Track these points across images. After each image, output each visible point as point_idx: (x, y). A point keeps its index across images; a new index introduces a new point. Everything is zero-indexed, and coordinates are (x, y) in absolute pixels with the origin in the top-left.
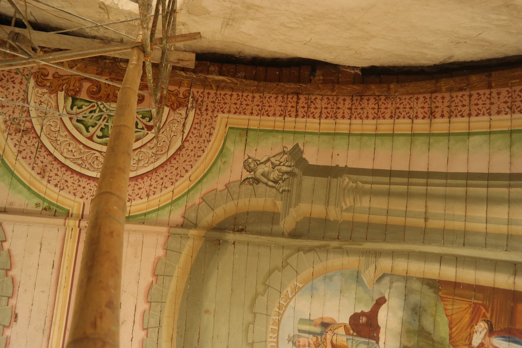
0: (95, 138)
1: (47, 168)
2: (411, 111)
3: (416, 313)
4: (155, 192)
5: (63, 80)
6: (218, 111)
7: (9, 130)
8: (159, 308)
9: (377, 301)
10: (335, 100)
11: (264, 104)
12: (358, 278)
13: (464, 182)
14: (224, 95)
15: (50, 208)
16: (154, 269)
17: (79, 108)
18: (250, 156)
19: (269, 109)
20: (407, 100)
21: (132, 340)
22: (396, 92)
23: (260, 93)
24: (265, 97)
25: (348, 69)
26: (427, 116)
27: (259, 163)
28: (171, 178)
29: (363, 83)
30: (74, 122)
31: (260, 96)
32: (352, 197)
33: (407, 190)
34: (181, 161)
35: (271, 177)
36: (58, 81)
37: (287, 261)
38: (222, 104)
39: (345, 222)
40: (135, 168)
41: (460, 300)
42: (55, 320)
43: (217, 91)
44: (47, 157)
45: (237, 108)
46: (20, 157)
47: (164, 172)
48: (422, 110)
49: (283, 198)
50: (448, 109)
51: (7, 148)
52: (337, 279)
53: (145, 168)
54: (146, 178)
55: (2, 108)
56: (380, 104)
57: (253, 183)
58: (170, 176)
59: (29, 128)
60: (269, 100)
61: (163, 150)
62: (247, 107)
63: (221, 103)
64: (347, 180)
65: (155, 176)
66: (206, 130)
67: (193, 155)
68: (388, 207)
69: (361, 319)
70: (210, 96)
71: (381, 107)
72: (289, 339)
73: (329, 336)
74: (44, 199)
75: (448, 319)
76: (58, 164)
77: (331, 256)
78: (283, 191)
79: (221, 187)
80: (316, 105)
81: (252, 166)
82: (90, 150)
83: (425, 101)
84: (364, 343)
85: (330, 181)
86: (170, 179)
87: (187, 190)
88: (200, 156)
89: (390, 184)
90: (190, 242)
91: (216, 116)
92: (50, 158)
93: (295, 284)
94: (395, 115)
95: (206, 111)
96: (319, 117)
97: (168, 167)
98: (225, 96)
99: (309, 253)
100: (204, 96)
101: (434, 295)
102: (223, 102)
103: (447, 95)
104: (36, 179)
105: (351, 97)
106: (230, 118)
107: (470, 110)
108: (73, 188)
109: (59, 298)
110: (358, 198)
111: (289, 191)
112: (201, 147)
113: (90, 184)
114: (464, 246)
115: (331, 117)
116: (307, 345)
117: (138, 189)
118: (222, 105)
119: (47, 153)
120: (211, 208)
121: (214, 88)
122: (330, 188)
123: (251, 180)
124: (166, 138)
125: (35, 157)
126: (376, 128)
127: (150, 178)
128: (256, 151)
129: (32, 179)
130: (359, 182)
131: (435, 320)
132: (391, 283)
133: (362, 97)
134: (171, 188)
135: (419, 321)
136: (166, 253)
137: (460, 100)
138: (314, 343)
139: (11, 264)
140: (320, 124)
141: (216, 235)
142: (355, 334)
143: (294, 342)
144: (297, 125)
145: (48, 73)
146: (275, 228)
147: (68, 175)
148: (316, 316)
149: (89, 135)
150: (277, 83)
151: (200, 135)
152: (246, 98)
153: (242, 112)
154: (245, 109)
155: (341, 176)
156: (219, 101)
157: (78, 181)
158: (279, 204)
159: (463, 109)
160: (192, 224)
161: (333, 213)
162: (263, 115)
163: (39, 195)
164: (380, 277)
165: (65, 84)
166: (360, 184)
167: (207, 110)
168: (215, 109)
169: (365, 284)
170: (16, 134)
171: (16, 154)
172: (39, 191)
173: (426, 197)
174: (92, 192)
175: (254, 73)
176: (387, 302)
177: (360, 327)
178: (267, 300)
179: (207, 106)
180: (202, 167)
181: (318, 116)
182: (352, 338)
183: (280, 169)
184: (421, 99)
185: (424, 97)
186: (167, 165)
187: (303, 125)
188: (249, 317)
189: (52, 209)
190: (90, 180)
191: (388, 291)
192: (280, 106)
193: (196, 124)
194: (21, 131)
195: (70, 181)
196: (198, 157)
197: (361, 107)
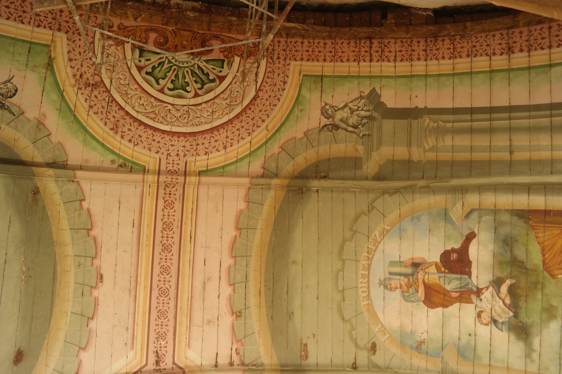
0: (166, 91)
1: (119, 123)
2: (488, 48)
3: (507, 244)
4: (232, 144)
5: (128, 32)
6: (290, 59)
7: (79, 84)
8: (244, 263)
9: (466, 236)
10: (409, 43)
11: (337, 51)
12: (446, 216)
13: (548, 112)
14: (295, 43)
15: (125, 165)
16: (237, 222)
17: (147, 60)
18: (327, 102)
19: (343, 55)
20: (483, 38)
22: (471, 31)
23: (331, 39)
24: (337, 43)
25: (420, 11)
26: (505, 52)
27: (336, 109)
28: (247, 129)
29: (436, 24)
30: (143, 73)
31: (332, 42)
32: (434, 137)
33: (489, 126)
34: (257, 111)
35: (351, 122)
36: (124, 32)
37: (373, 204)
38: (294, 51)
39: (429, 162)
40: (210, 120)
41: (552, 227)
42: (140, 280)
43: (287, 38)
44: (119, 112)
45: (309, 55)
46: (91, 113)
47: (240, 122)
48: (500, 47)
49: (364, 142)
50: (526, 43)
51: (78, 103)
52: (425, 219)
53: (220, 120)
54: (221, 130)
55: (71, 62)
56: (455, 44)
57: (332, 129)
58: (246, 127)
59: (99, 82)
60: (342, 46)
61: (237, 100)
62: (320, 54)
63: (292, 51)
64: (428, 120)
65: (231, 128)
66: (280, 78)
67: (268, 104)
68: (471, 144)
69: (452, 255)
70: (281, 44)
71: (457, 47)
72: (380, 283)
73: (420, 276)
74: (119, 156)
75: (540, 246)
76: (130, 118)
77: (417, 196)
78: (364, 135)
79: (300, 135)
80: (390, 49)
81: (330, 112)
82: (162, 103)
83: (502, 37)
84: (457, 279)
85: (411, 122)
86: (246, 129)
87: (265, 140)
88: (276, 105)
89: (472, 121)
90: (272, 193)
91: (288, 64)
92: (122, 113)
93: (383, 227)
94: (472, 53)
95: (278, 60)
96: (394, 60)
97: (244, 118)
98: (296, 44)
99: (394, 196)
100: (274, 45)
101: (524, 225)
102: (295, 49)
103: (525, 30)
104: (109, 134)
105: (425, 39)
106: (303, 66)
107: (550, 42)
108: (147, 143)
109: (142, 257)
110: (440, 137)
111: (369, 135)
112: (276, 96)
114: (552, 174)
115: (407, 60)
116: (399, 287)
117: (215, 141)
118: (294, 53)
120: (291, 156)
121: (284, 36)
122: (410, 129)
123: (330, 126)
124: (239, 88)
125: (107, 112)
126: (453, 67)
127: (226, 129)
128: (332, 97)
129: (105, 135)
130: (440, 122)
131: (527, 249)
132: (480, 217)
133: (437, 38)
134: (248, 139)
135: (511, 252)
137: (539, 33)
138: (406, 284)
140: (395, 67)
141: (299, 182)
142: (447, 271)
143: (385, 285)
144: (373, 69)
145: (113, 24)
146: (358, 173)
147: (142, 130)
148: (407, 257)
149: (159, 87)
150: (349, 28)
151: (274, 83)
152: (317, 45)
153: (315, 59)
154: (318, 55)
155: (421, 117)
156: (291, 49)
157: (152, 135)
158: (361, 148)
159: (543, 42)
160: (273, 175)
161: (416, 154)
162: (337, 61)
163: (114, 151)
164: (468, 213)
165: (131, 35)
166: (441, 124)
167: (278, 58)
168: (287, 57)
169: (454, 221)
170: (86, 88)
171: (88, 109)
172: (114, 147)
173: (510, 130)
175: (323, 19)
176: (477, 237)
177: (452, 263)
178: (355, 246)
179: (279, 54)
180: (279, 116)
181: (393, 59)
182: (444, 275)
183: (359, 114)
184: (498, 36)
185: (501, 34)
186: (242, 115)
187: (378, 69)
188: (339, 265)
189: (127, 166)
190: (165, 134)
191: (477, 226)
192: (354, 51)
193: (268, 72)
194: (91, 85)
195: (144, 136)
196: (274, 105)
197: (436, 48)
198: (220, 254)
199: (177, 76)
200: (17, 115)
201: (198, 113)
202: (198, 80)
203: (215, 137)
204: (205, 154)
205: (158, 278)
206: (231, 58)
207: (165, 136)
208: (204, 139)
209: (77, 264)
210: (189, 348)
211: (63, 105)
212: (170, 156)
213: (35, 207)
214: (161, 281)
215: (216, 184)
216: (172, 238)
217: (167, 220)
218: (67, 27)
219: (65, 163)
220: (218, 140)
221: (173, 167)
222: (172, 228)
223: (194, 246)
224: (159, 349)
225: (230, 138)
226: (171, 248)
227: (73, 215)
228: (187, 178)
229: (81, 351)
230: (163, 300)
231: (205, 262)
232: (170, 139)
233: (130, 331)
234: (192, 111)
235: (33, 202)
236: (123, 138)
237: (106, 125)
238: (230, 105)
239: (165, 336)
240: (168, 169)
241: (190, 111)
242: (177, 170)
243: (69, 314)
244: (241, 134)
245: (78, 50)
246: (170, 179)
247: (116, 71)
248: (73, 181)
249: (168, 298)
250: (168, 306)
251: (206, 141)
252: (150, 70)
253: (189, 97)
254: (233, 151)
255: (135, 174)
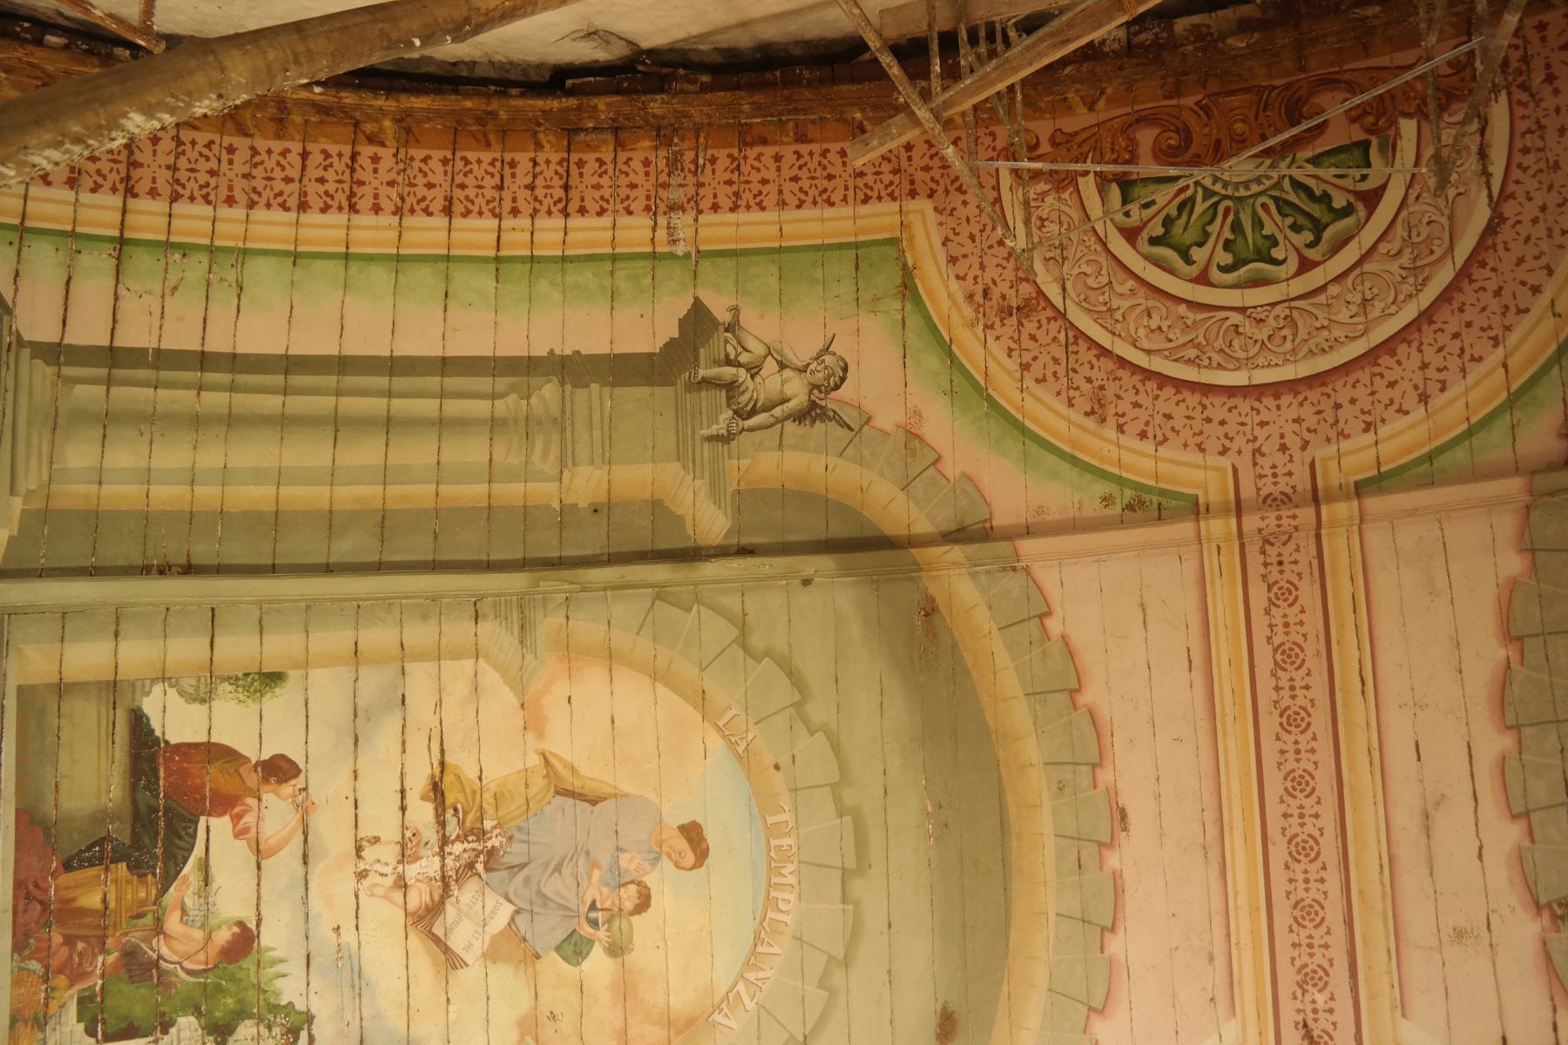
0: (1216, 275)
15: (1142, 503)
17: (1146, 206)
21: (1480, 857)
30: (1145, 247)
40: (1361, 327)
42: (1231, 816)
47: (1456, 313)
51: (992, 364)
53: (1393, 318)
54: (1402, 349)
58: (1480, 320)
61: (1434, 248)
74: (1120, 481)
76: (1133, 374)
87: (1554, 347)
92: (1107, 364)
97: (1468, 295)
104: (1085, 430)
109: (1226, 752)
113: (1236, 407)
117: (1387, 387)
119: (1094, 352)
124: (1434, 210)
127: (1415, 344)
134: (1495, 357)
136: (1534, 562)
139: (1078, 675)
149: (1194, 270)
157: (1199, 408)
172: (1102, 460)
174: (1247, 429)
186: (1460, 290)
190: (1235, 396)
195: (1179, 413)
198: (1464, 721)
199: (1237, 227)
200: (856, 429)
201: (1321, 314)
202: (1301, 220)
203: (1387, 373)
204: (1366, 430)
205: (1282, 808)
206: (1389, 128)
207: (1238, 401)
208: (1354, 386)
209: (1054, 786)
210: (1404, 1015)
211: (957, 378)
212: (1263, 455)
213: (934, 649)
214: (1292, 816)
215: (1412, 513)
216: (1307, 687)
217: (1285, 639)
218: (928, 181)
219: (987, 525)
220: (1396, 382)
221: (1275, 484)
222: (1304, 660)
223: (1377, 706)
224: (1310, 1016)
225: (1432, 367)
226: (1307, 719)
227: (1027, 657)
228: (1324, 508)
229: (1093, 1017)
230: (1306, 871)
231: (1417, 749)
232: (1252, 409)
233: (1220, 963)
234: (1305, 315)
235: (927, 635)
236: (1123, 432)
237: (1073, 405)
238: (1413, 270)
239: (1325, 978)
240: (1264, 493)
241: (1295, 314)
242: (1289, 491)
243: (1052, 917)
244: (1467, 347)
245: (965, 231)
246: (1272, 521)
247: (1071, 258)
248: (1014, 569)
249: (1318, 864)
250: (1323, 887)
251: (1361, 393)
252: (1160, 231)
253: (1284, 276)
254: (1451, 402)
255: (1172, 523)
